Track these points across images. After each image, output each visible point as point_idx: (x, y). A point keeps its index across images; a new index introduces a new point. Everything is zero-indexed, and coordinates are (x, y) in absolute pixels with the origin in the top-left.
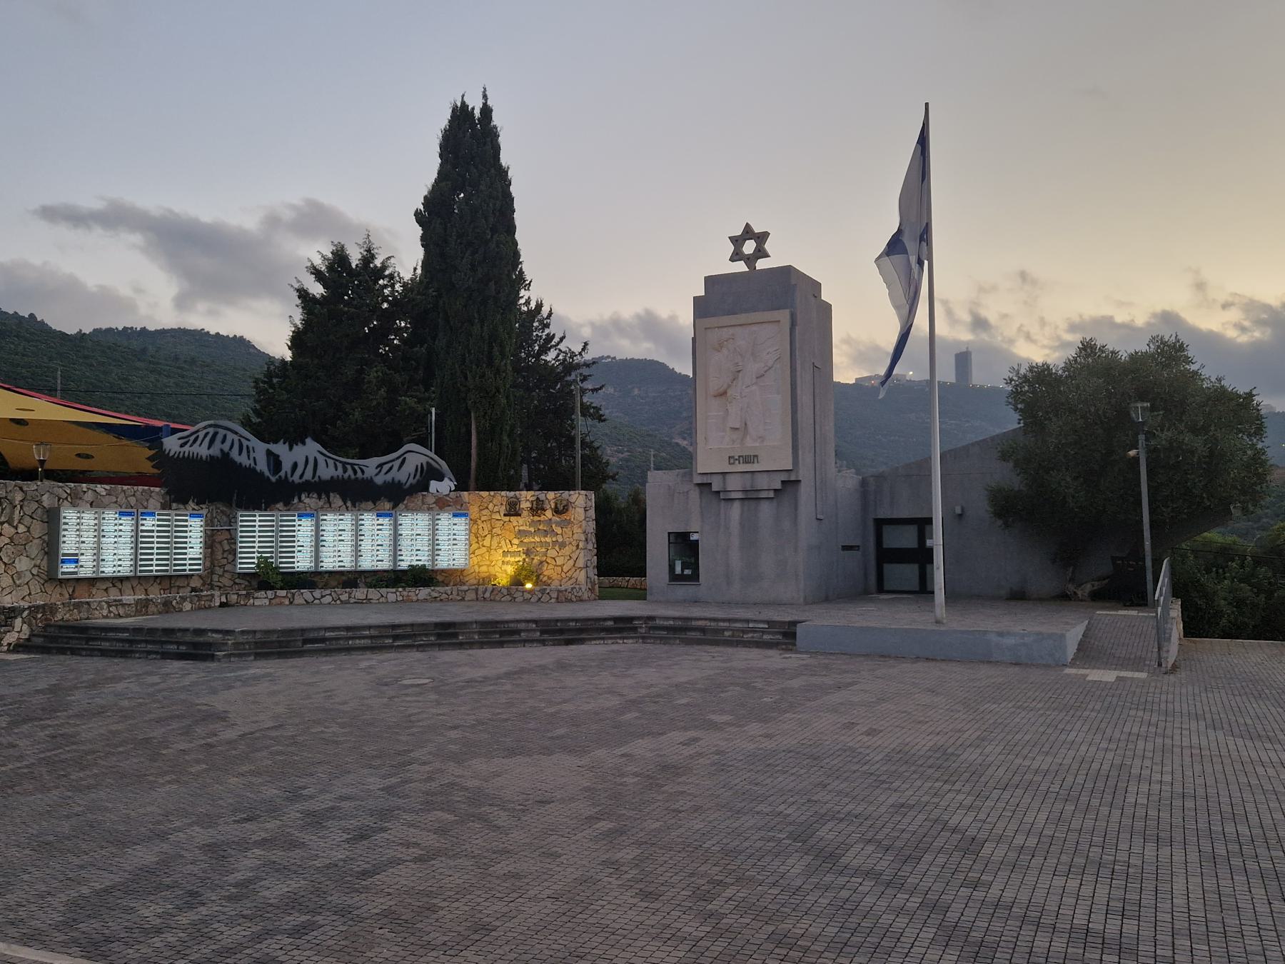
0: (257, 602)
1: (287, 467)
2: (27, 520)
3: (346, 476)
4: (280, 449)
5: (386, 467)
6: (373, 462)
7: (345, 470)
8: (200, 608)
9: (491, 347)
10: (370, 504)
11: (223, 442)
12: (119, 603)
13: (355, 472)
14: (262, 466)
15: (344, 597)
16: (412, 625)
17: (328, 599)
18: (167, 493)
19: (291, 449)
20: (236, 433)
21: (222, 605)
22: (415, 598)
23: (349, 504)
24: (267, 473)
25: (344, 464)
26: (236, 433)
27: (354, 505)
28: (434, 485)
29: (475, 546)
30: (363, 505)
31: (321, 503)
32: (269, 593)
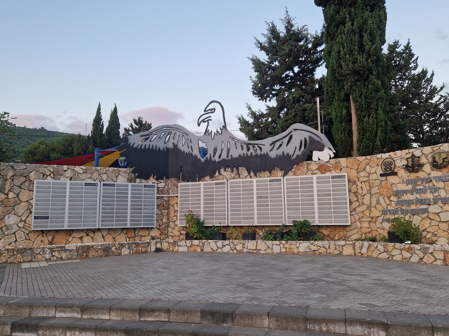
0: (181, 249)
1: (210, 152)
2: (17, 190)
5: (277, 144)
7: (248, 149)
8: (137, 253)
9: (362, 37)
10: (267, 172)
12: (63, 249)
14: (196, 152)
15: (239, 247)
16: (168, 311)
21: (158, 250)
24: (199, 156)
27: (256, 175)
28: (316, 155)
29: (356, 204)
30: (262, 174)
31: (233, 175)
32: (188, 242)
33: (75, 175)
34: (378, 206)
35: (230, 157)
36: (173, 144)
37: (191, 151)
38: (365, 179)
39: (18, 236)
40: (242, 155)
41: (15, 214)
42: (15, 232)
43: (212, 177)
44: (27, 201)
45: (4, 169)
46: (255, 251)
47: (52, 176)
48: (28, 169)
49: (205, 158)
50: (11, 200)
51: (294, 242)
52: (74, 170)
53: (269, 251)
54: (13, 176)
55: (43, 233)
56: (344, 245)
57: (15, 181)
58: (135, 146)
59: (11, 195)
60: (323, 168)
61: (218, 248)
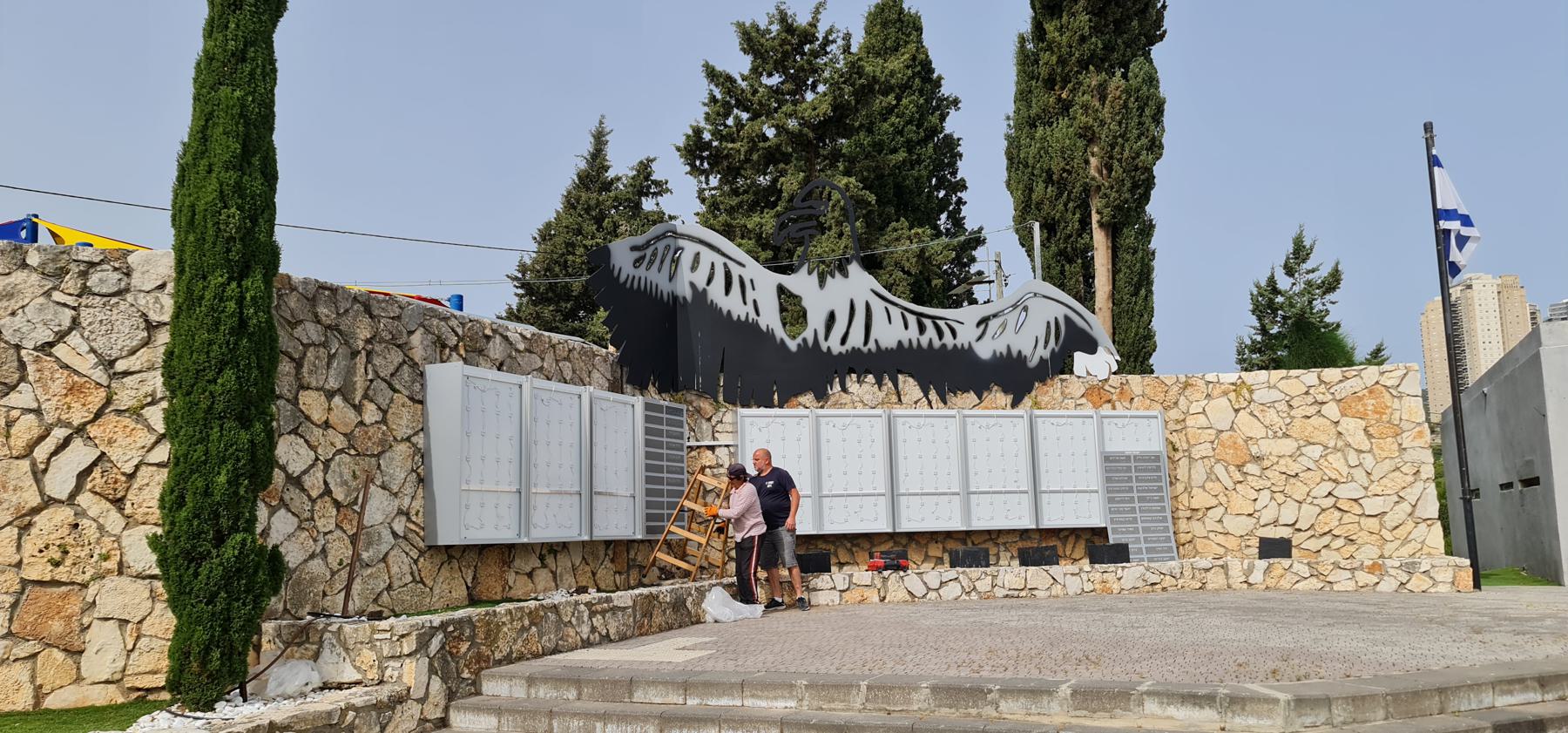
1: (816, 321)
3: (924, 341)
4: (801, 283)
6: (966, 316)
7: (922, 329)
11: (694, 268)
13: (940, 334)
14: (770, 319)
15: (984, 585)
17: (952, 591)
18: (621, 361)
19: (822, 283)
20: (718, 251)
22: (1116, 587)
23: (933, 395)
24: (780, 333)
25: (919, 315)
26: (718, 251)
28: (1081, 360)
31: (881, 395)
33: (510, 356)
34: (1209, 485)
35: (872, 345)
36: (692, 285)
37: (752, 315)
38: (1179, 427)
39: (395, 569)
40: (906, 344)
41: (384, 487)
42: (387, 554)
43: (822, 396)
44: (408, 439)
45: (347, 311)
46: (1023, 594)
47: (462, 352)
48: (405, 320)
49: (799, 340)
50: (371, 430)
51: (1112, 567)
52: (506, 338)
53: (1057, 590)
54: (368, 341)
55: (450, 557)
56: (1207, 570)
57: (377, 361)
58: (622, 279)
59: (371, 414)
60: (1097, 393)
61: (929, 589)
